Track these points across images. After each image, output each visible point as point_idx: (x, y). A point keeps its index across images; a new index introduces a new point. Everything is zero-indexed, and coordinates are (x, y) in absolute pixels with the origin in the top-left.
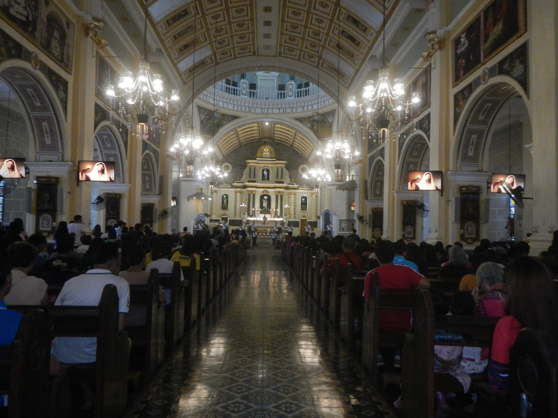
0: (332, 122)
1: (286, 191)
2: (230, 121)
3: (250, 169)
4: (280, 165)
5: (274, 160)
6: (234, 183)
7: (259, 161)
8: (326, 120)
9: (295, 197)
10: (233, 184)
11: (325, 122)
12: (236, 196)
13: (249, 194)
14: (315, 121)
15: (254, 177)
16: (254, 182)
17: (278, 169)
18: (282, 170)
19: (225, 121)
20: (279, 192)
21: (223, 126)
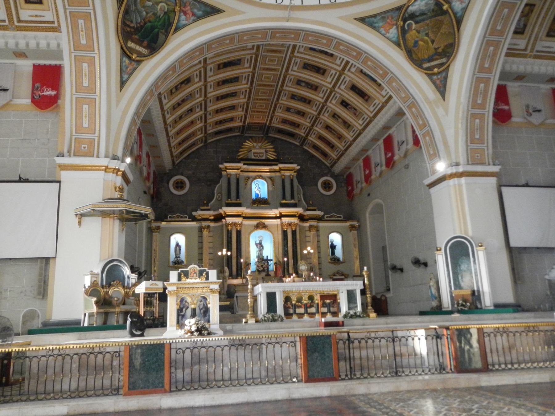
0: (465, 10)
1: (302, 224)
2: (199, 18)
3: (229, 180)
4: (287, 173)
5: (277, 165)
6: (196, 211)
7: (245, 166)
8: (445, 7)
9: (318, 236)
10: (194, 213)
11: (445, 13)
12: (201, 237)
13: (228, 231)
14: (412, 16)
15: (238, 197)
16: (239, 205)
17: (283, 181)
18: (292, 181)
19: (185, 13)
20: (290, 224)
21: (177, 29)
